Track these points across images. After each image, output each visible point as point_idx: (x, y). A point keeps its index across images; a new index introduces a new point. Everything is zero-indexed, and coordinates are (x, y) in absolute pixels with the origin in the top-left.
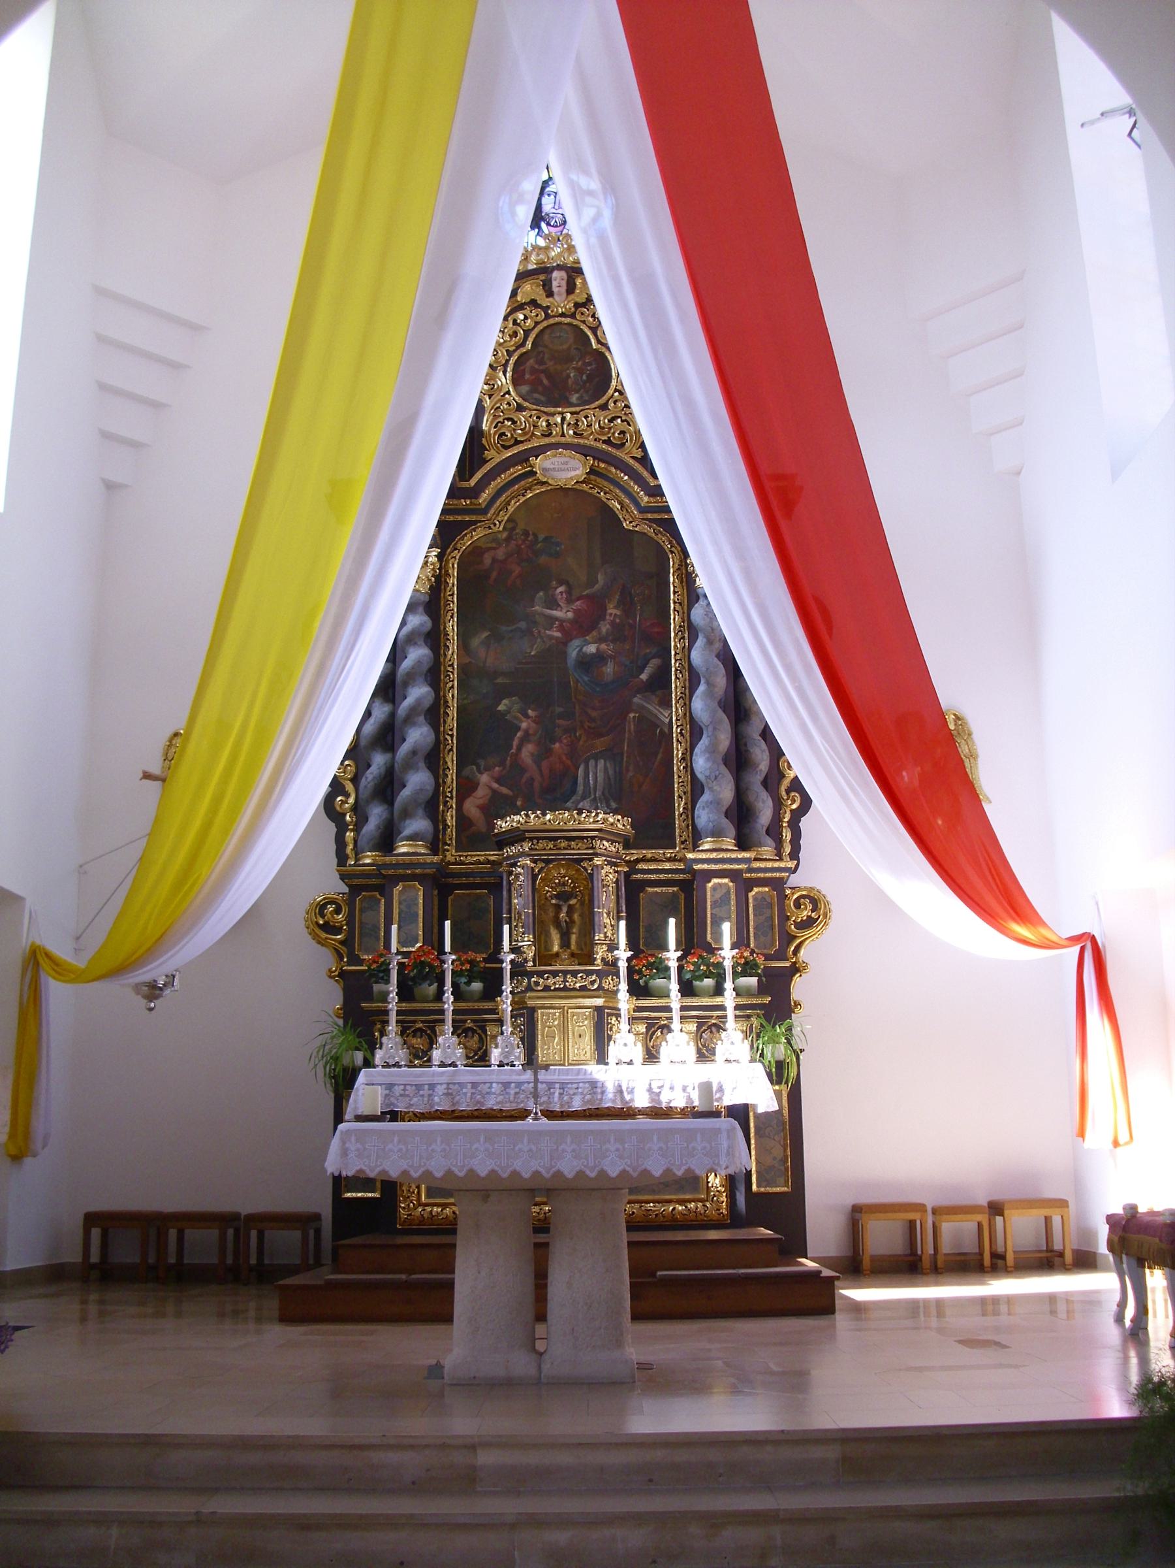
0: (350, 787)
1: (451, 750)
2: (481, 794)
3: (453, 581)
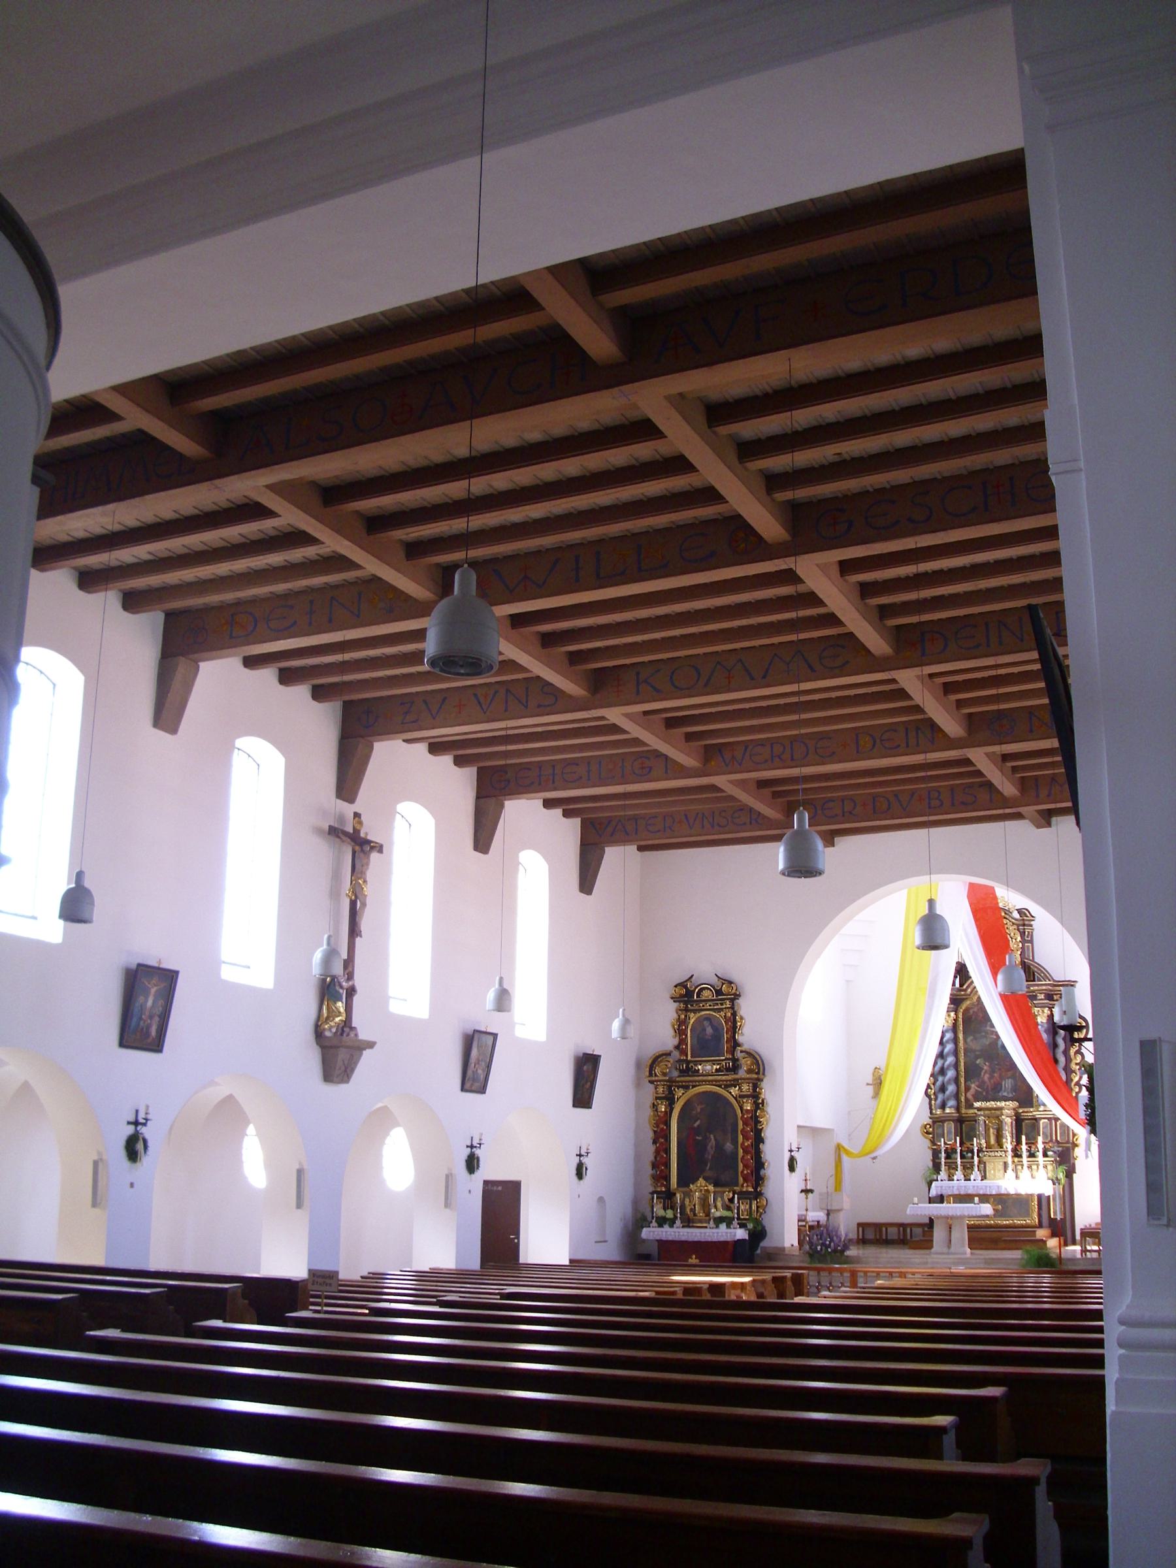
2: (972, 1091)
3: (960, 1020)
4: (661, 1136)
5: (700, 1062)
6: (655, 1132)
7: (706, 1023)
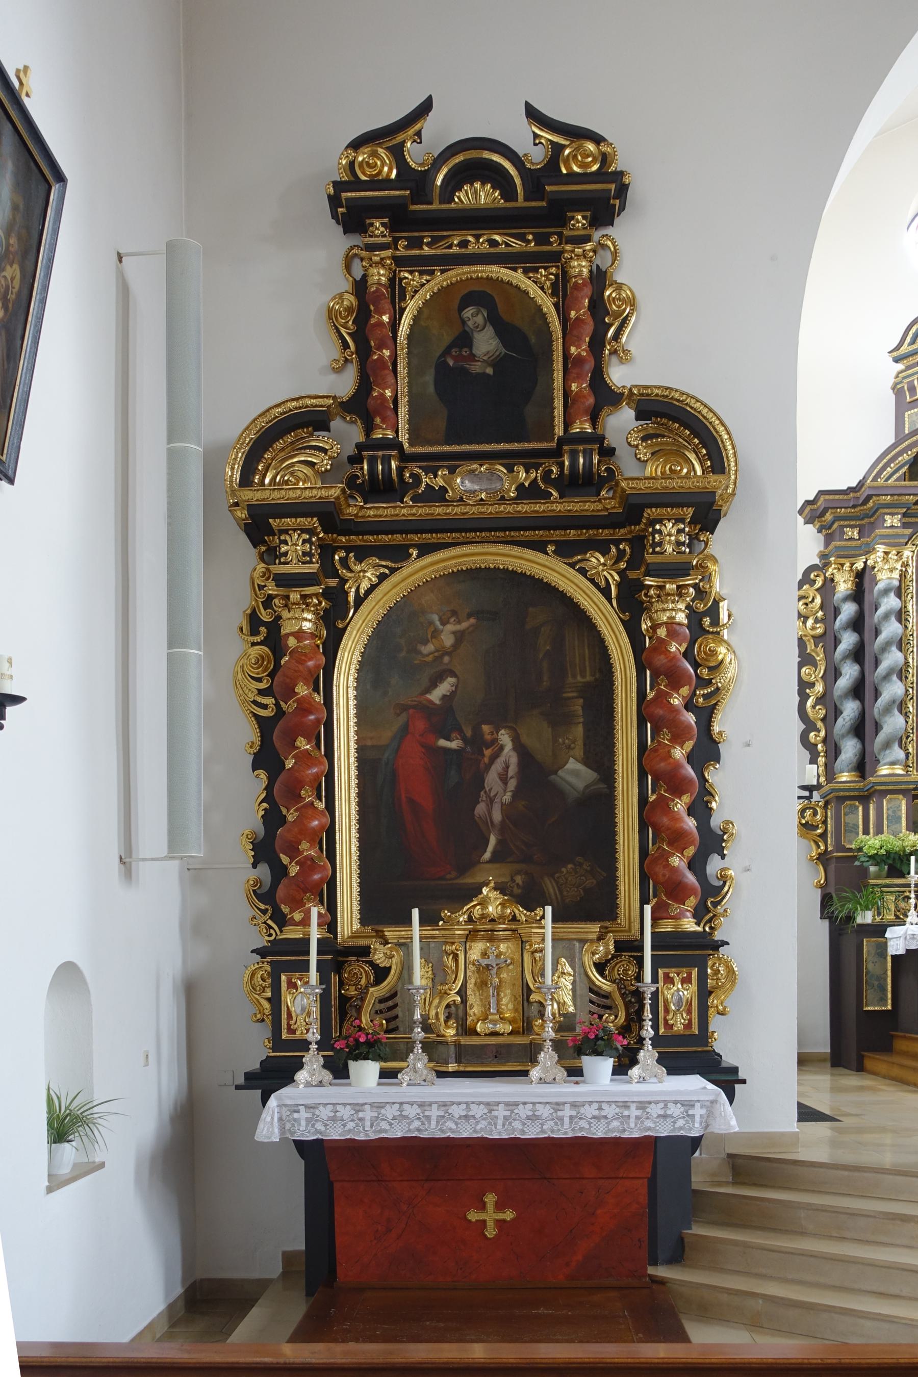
0: (820, 724)
1: (912, 698)
4: (282, 743)
5: (453, 461)
6: (265, 726)
7: (473, 316)
